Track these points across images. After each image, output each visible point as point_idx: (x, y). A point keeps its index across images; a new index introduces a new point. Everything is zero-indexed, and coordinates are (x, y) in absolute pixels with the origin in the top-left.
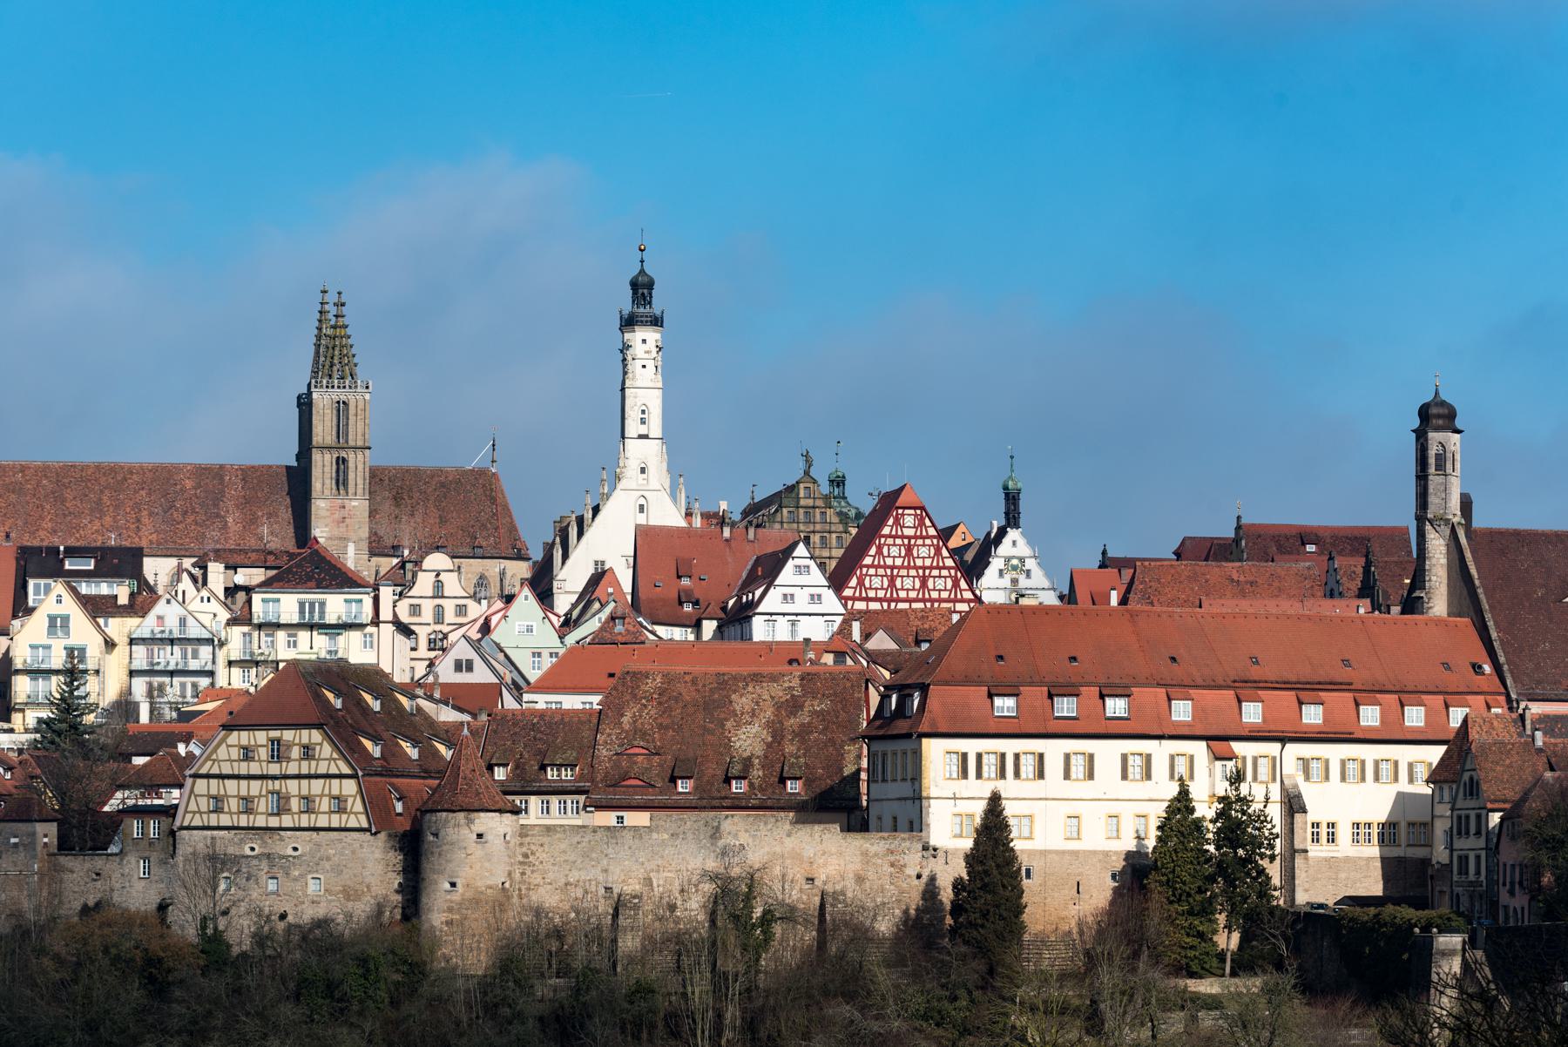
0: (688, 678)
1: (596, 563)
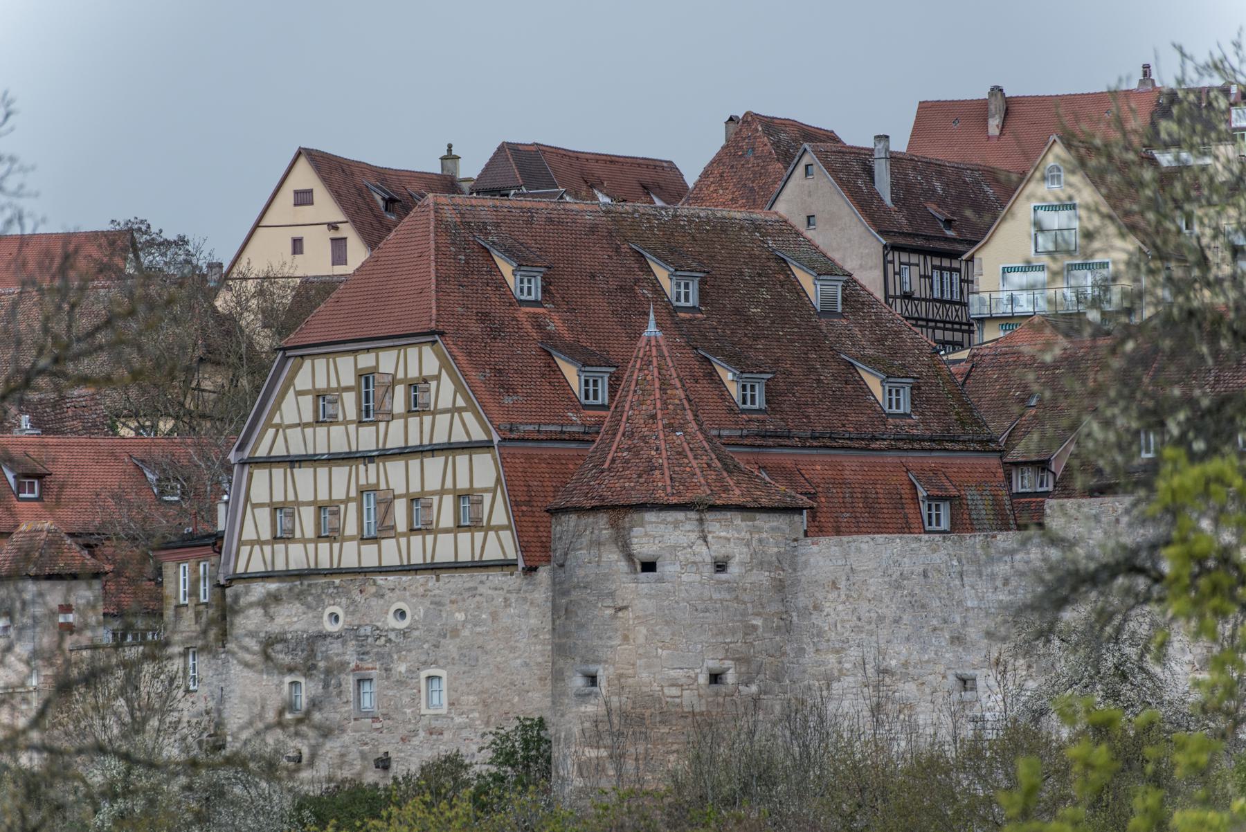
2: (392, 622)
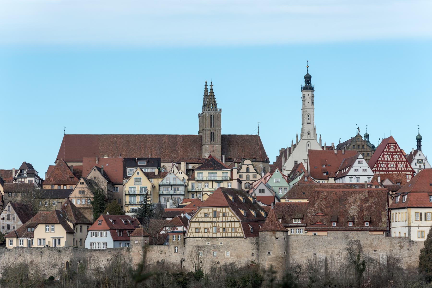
0: (334, 192)
1: (295, 162)
2: (220, 244)
